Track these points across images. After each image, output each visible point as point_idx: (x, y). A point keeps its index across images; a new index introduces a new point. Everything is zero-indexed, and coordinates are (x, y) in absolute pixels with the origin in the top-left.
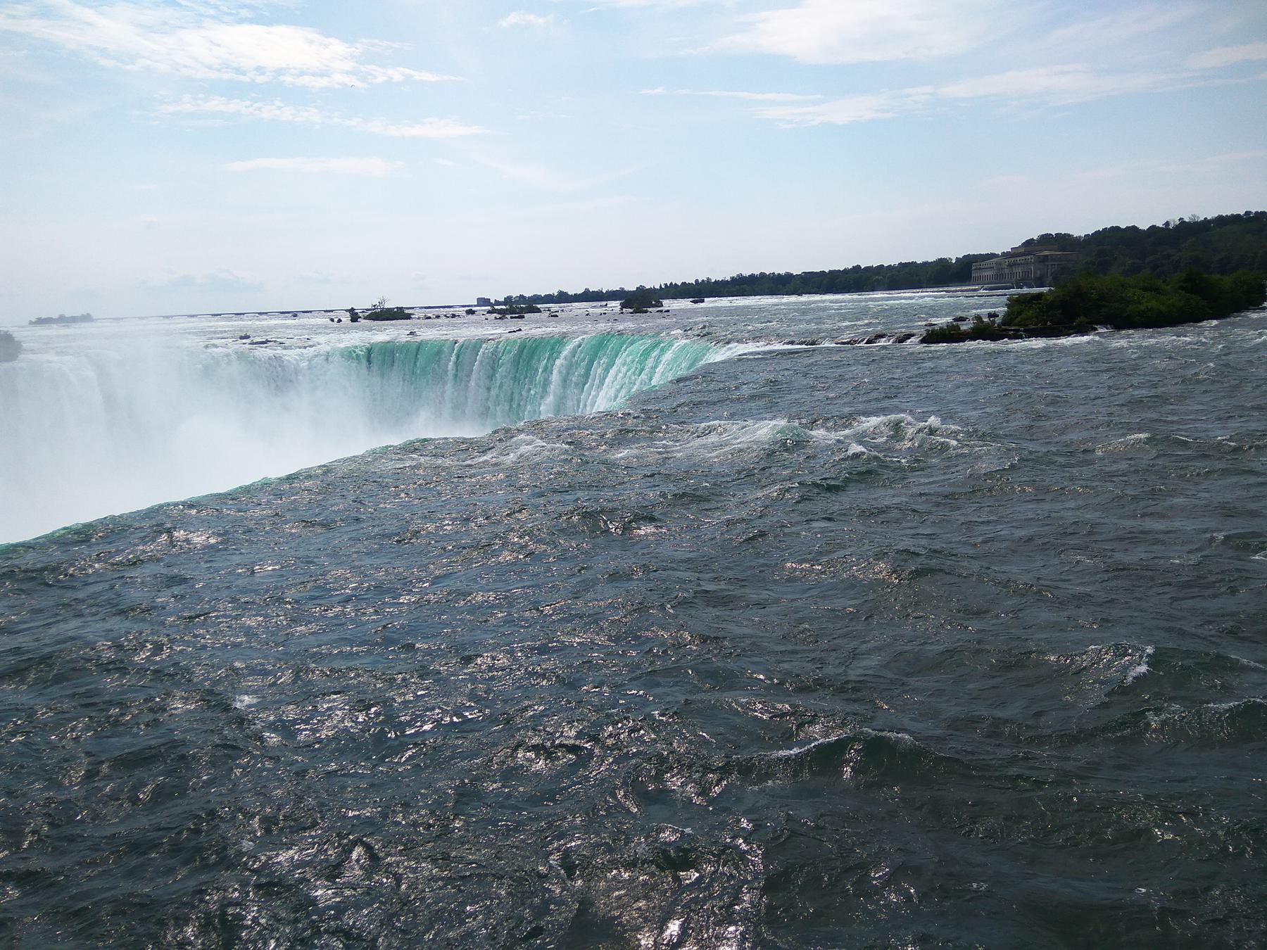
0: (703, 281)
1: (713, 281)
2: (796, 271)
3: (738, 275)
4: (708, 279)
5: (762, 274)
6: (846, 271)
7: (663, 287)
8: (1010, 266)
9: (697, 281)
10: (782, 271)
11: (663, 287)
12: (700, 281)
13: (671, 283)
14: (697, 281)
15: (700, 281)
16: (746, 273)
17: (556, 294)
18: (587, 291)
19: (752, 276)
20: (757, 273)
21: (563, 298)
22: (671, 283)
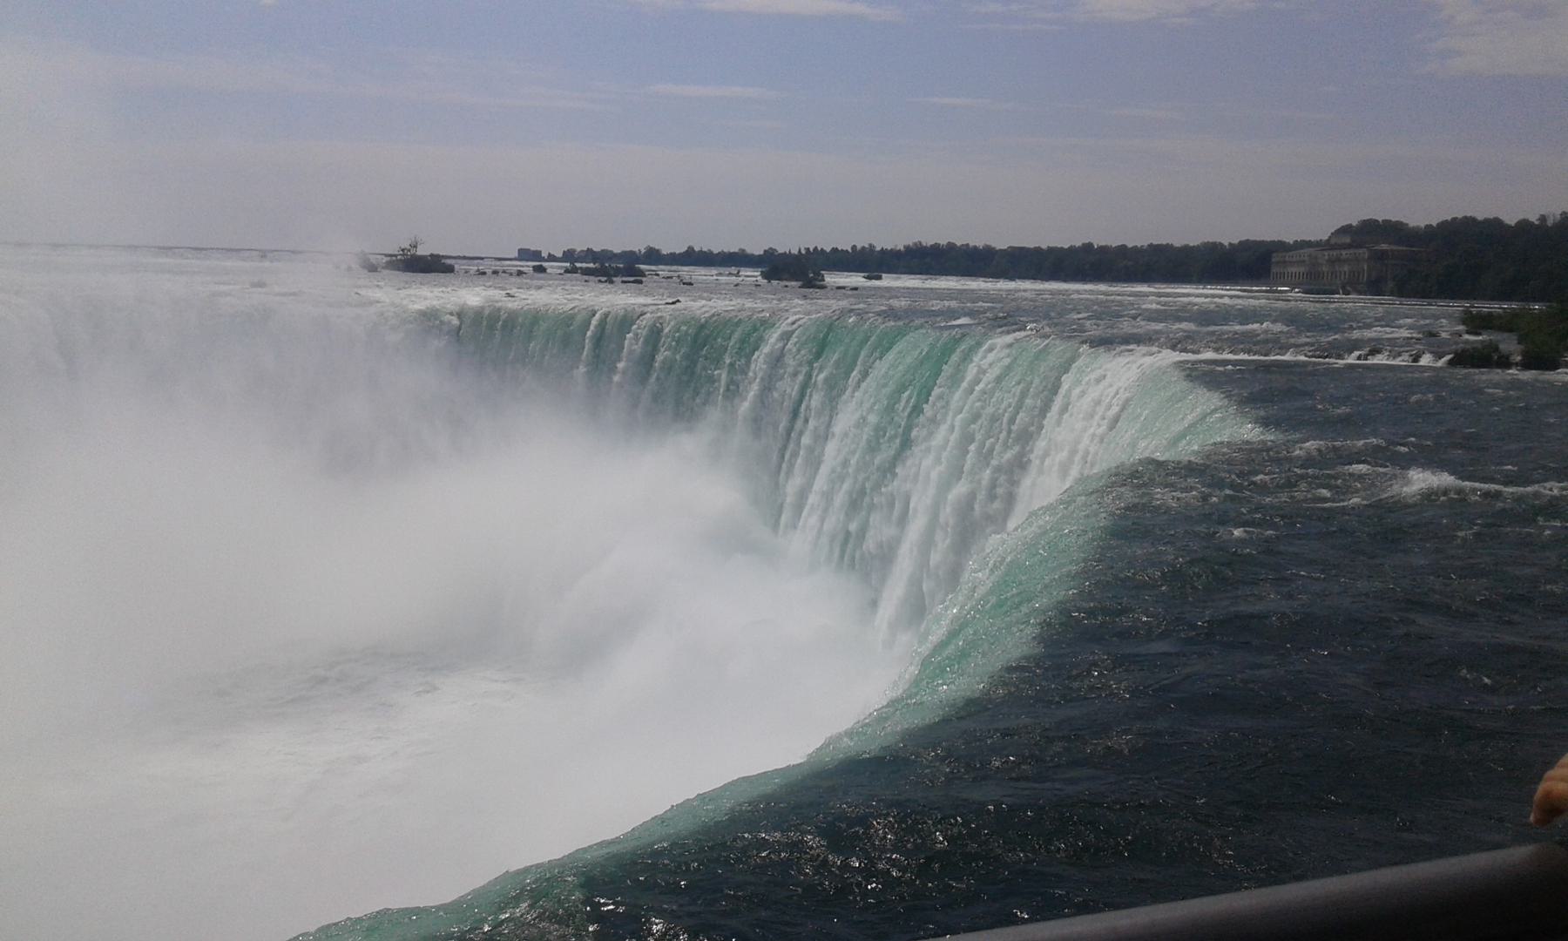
0: (863, 248)
1: (878, 249)
2: (1001, 244)
3: (915, 244)
4: (870, 245)
5: (951, 246)
6: (1072, 250)
7: (803, 252)
8: (1332, 262)
9: (854, 247)
10: (978, 241)
11: (803, 252)
12: (859, 247)
13: (816, 248)
14: (854, 247)
15: (859, 247)
16: (928, 241)
17: (643, 251)
18: (690, 251)
19: (936, 247)
20: (943, 242)
21: (653, 256)
22: (816, 248)
